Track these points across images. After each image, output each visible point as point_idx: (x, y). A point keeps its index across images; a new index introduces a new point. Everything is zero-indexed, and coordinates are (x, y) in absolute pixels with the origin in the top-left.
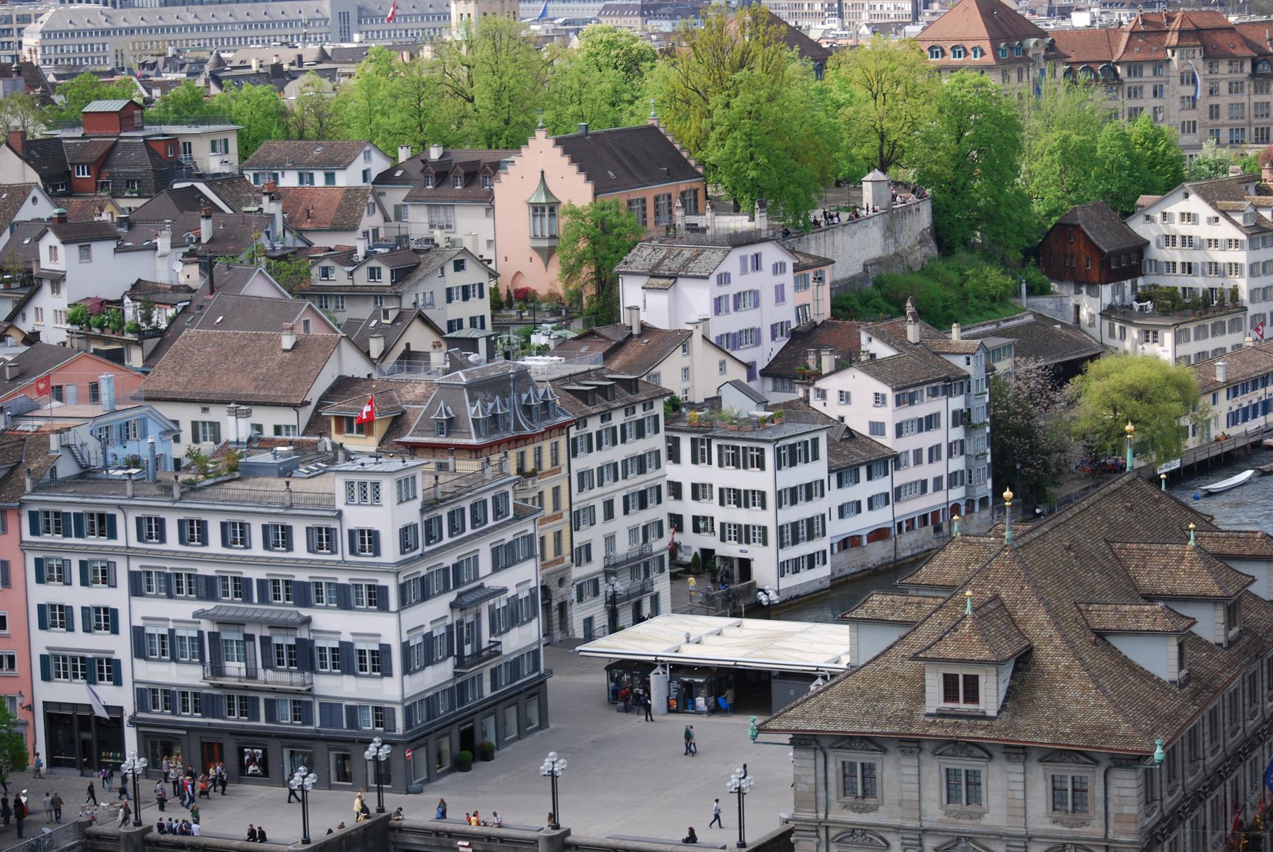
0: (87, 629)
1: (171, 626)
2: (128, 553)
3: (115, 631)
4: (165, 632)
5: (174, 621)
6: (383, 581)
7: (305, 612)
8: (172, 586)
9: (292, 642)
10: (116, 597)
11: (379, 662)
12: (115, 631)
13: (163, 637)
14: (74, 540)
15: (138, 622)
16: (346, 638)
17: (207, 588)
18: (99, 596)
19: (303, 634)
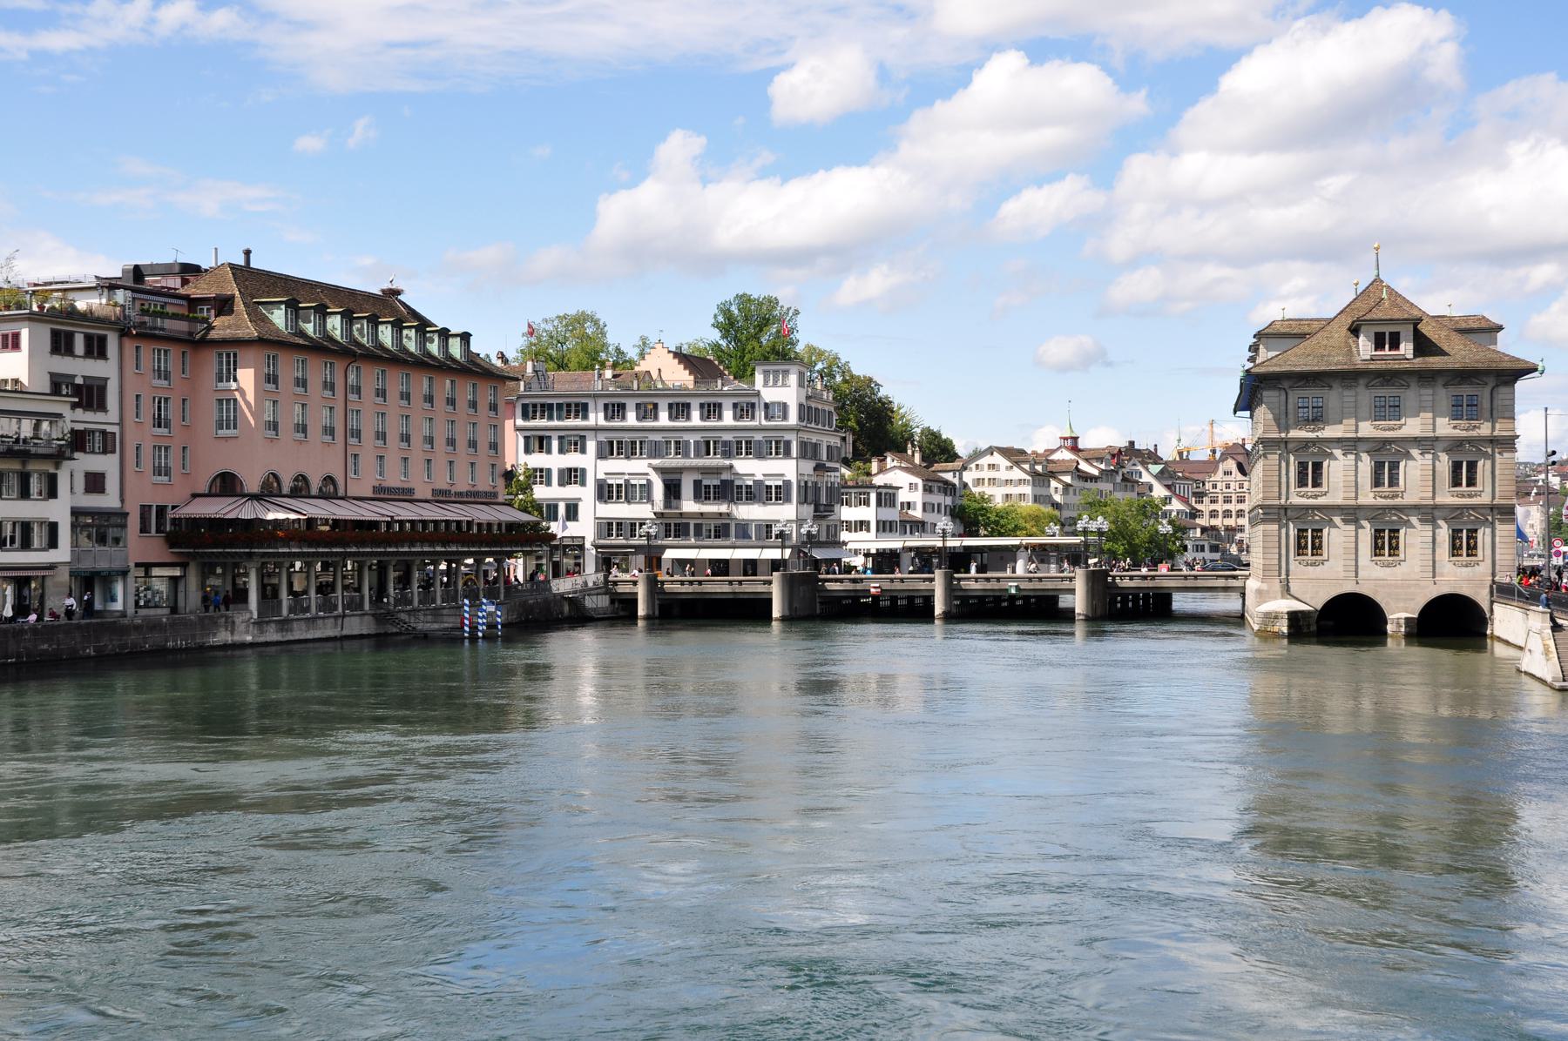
0: (561, 484)
1: (627, 477)
2: (596, 430)
3: (583, 484)
4: (621, 482)
5: (629, 474)
6: (787, 436)
7: (727, 462)
8: (628, 449)
9: (717, 482)
10: (585, 460)
11: (780, 494)
12: (583, 484)
13: (619, 486)
14: (555, 423)
15: (601, 476)
16: (759, 477)
17: (656, 451)
18: (573, 460)
19: (725, 476)
